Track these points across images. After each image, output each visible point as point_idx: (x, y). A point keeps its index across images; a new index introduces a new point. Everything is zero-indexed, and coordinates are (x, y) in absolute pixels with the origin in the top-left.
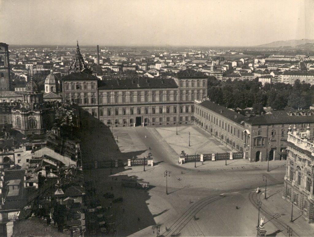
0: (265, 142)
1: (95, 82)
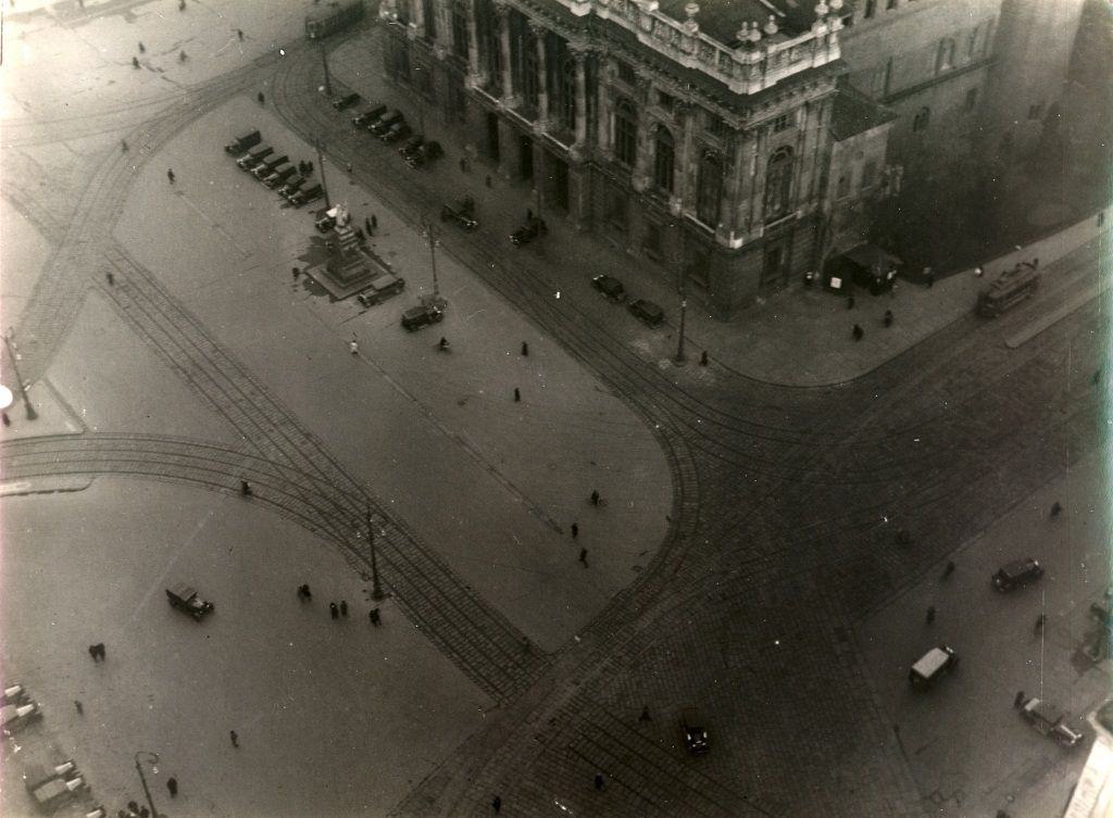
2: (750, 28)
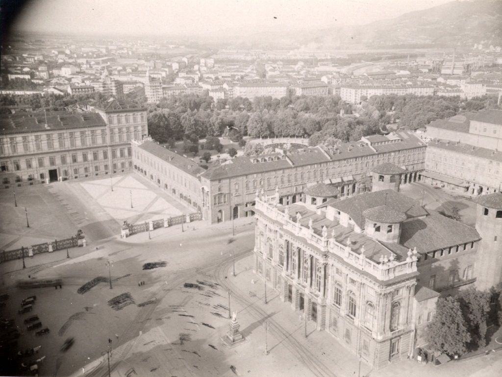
0: (228, 198)
2: (384, 257)
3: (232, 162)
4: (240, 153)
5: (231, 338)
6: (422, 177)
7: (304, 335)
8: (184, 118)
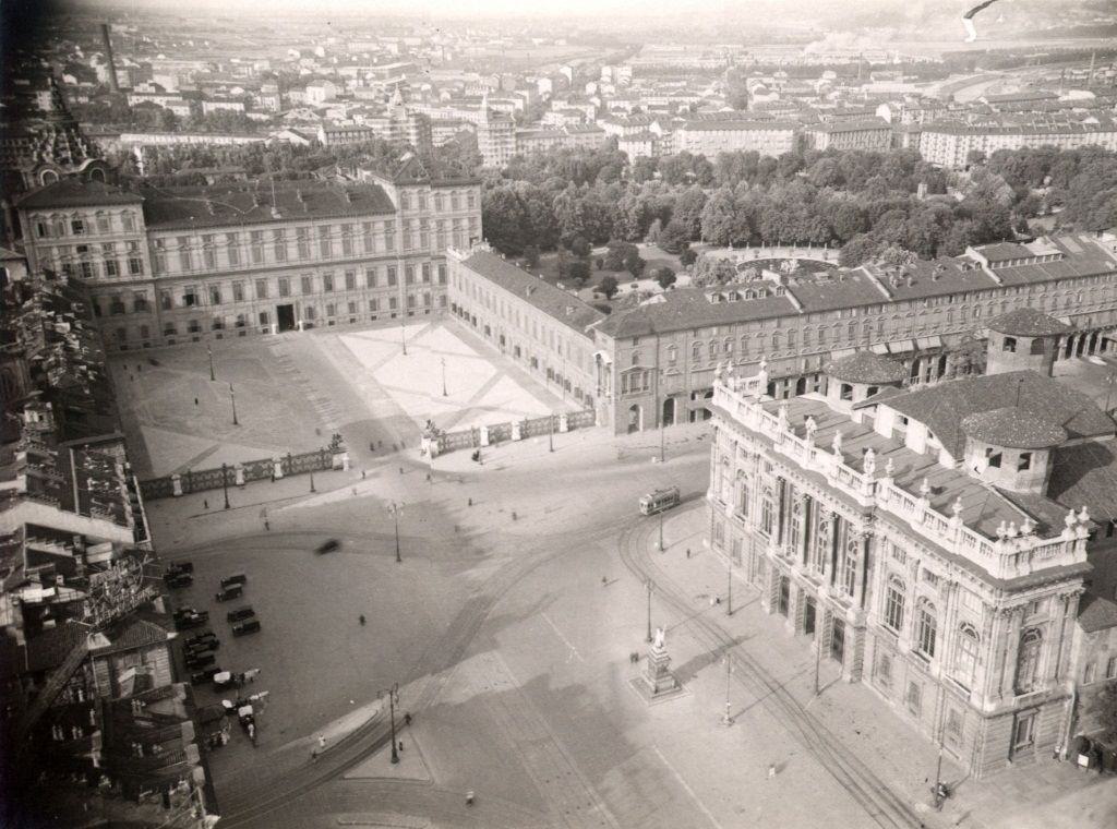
1: (135, 210)
2: (1007, 526)
3: (663, 300)
4: (683, 280)
5: (651, 684)
6: (1109, 344)
7: (812, 689)
8: (560, 202)
